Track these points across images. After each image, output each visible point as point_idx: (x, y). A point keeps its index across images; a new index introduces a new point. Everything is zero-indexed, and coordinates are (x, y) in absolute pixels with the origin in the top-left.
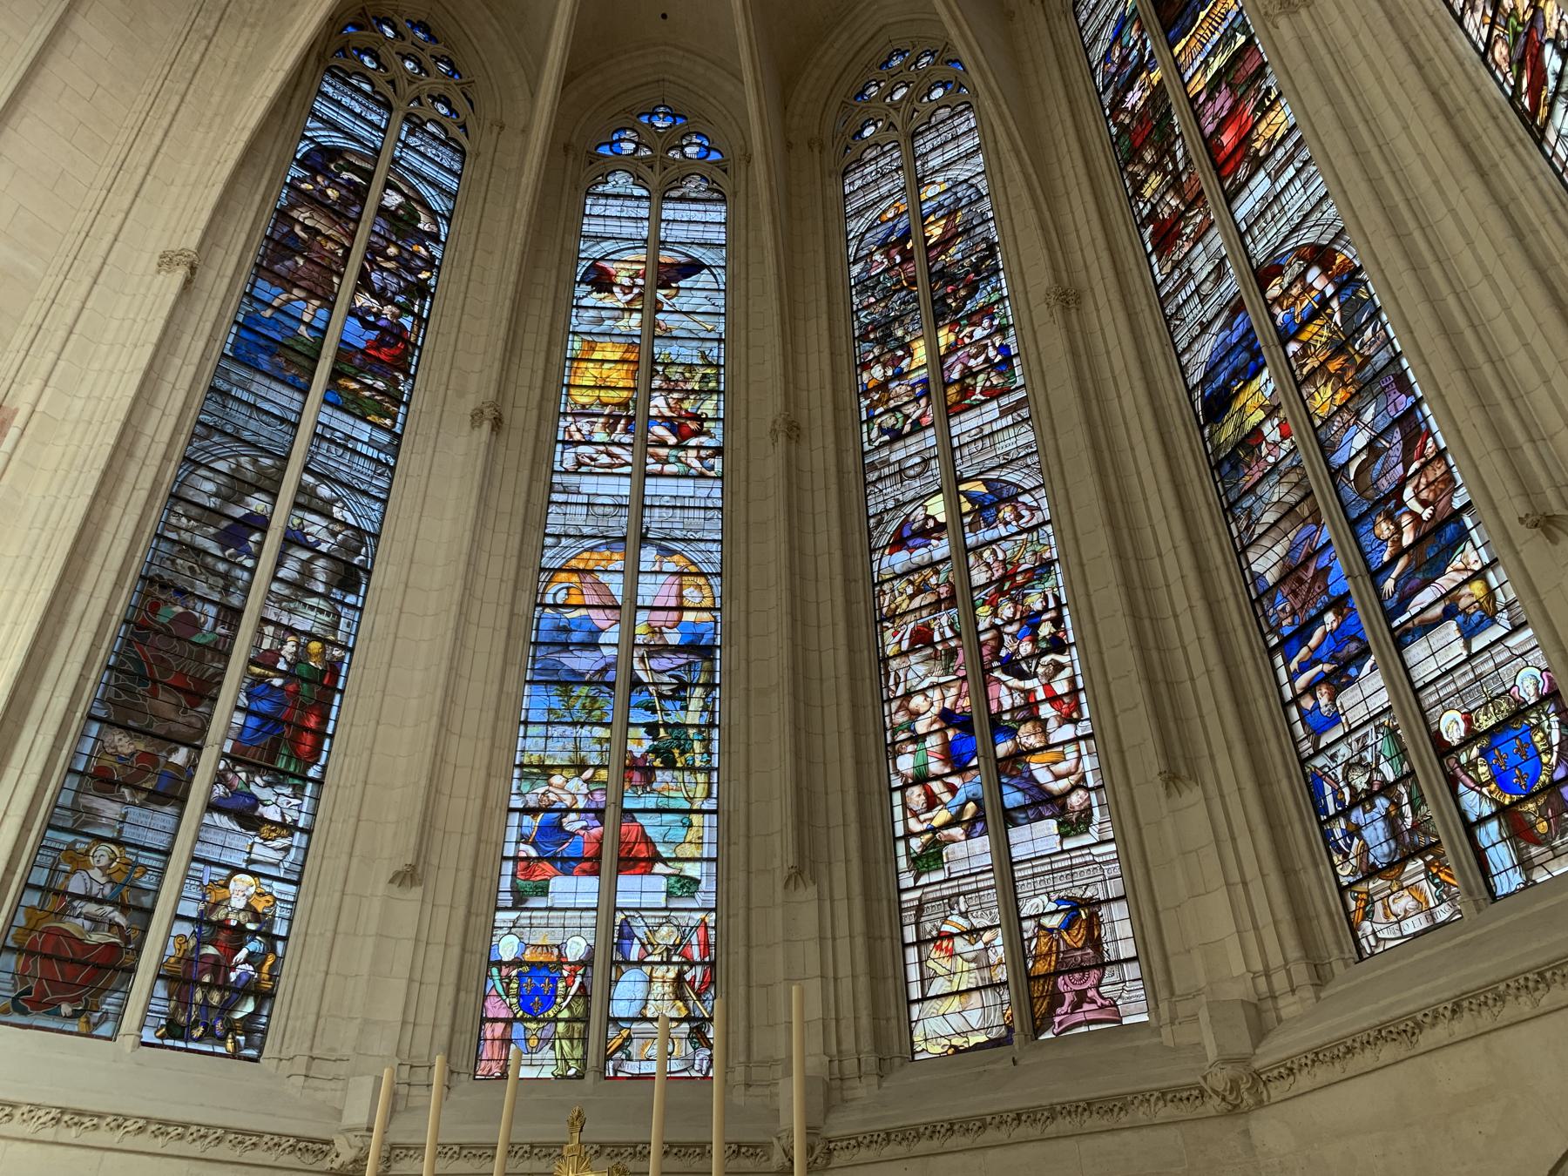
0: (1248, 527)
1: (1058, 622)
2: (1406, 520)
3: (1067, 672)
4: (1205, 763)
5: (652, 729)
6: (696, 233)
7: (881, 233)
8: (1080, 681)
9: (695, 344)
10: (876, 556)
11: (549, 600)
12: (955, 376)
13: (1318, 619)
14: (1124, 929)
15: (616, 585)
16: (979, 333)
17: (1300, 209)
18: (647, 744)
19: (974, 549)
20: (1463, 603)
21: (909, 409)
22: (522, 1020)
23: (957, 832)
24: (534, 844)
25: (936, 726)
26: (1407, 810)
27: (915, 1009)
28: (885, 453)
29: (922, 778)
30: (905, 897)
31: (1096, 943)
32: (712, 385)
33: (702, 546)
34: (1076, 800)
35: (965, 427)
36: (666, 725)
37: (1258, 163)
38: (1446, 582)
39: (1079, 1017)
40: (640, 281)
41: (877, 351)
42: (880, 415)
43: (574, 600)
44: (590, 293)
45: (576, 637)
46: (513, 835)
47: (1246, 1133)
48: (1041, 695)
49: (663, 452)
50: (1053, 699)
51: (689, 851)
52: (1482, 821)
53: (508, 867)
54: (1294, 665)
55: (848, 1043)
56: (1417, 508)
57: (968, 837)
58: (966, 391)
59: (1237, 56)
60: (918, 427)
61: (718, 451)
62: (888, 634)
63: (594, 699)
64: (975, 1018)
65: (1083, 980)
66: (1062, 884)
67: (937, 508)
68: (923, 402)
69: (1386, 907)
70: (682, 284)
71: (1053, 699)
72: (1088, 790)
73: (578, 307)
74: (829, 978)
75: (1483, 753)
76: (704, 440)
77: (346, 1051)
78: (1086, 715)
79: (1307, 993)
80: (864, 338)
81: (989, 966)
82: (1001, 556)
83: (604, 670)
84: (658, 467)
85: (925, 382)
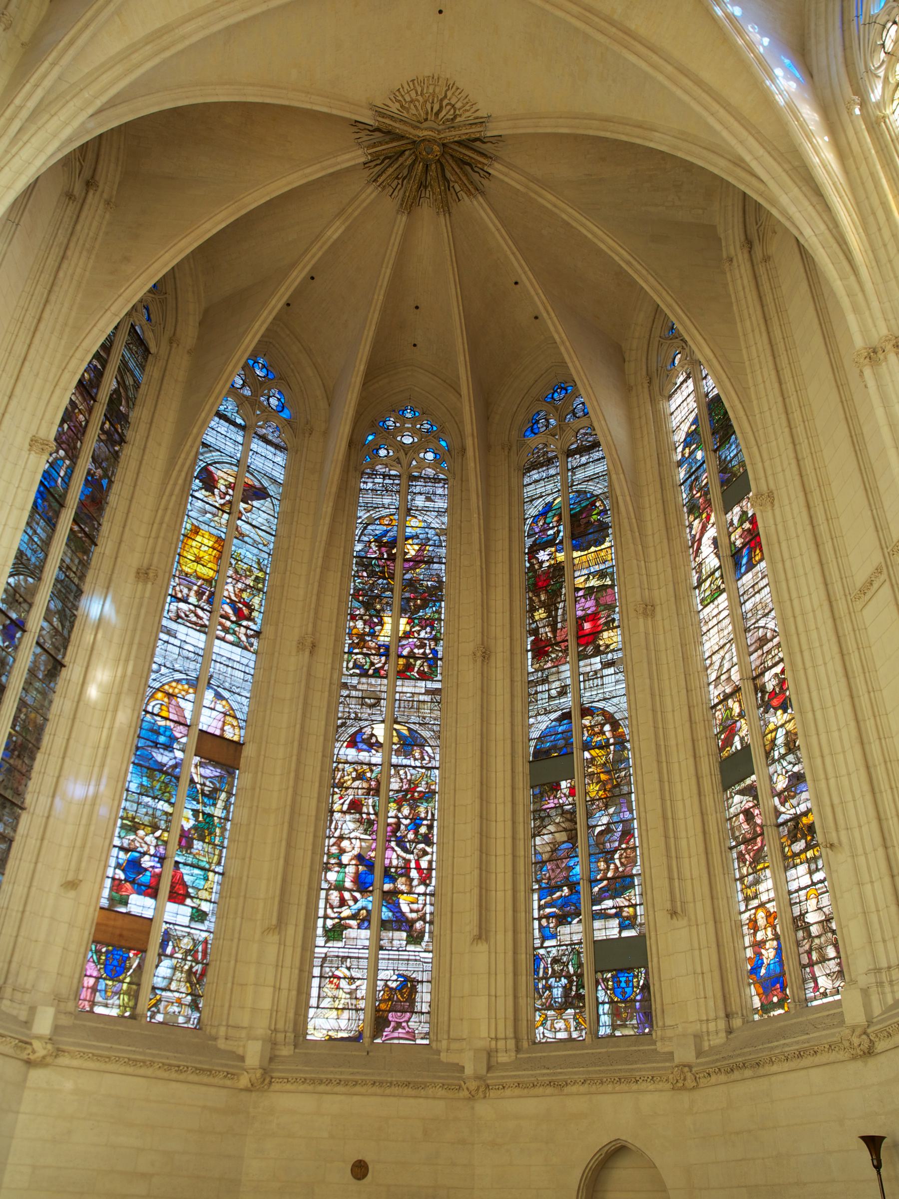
1: (430, 827)
2: (612, 866)
3: (428, 857)
4: (492, 934)
5: (196, 813)
6: (268, 467)
7: (379, 530)
8: (434, 865)
9: (256, 551)
10: (338, 745)
11: (150, 709)
12: (405, 653)
13: (559, 888)
14: (427, 997)
15: (188, 707)
16: (423, 634)
18: (192, 822)
19: (395, 766)
20: (625, 914)
21: (375, 659)
22: (105, 979)
23: (354, 923)
24: (123, 870)
25: (354, 862)
26: (574, 988)
27: (312, 1012)
28: (355, 681)
29: (339, 887)
30: (317, 950)
31: (412, 1002)
32: (260, 586)
33: (239, 698)
34: (418, 925)
35: (405, 689)
36: (204, 813)
37: (597, 652)
38: (621, 902)
39: (396, 1035)
40: (231, 492)
41: (362, 611)
42: (356, 654)
43: (164, 714)
44: (201, 489)
45: (162, 739)
46: (113, 862)
47: (473, 1108)
48: (413, 865)
49: (228, 624)
50: (418, 867)
51: (204, 894)
52: (603, 1003)
53: (108, 883)
54: (542, 902)
55: (280, 1025)
56: (618, 864)
57: (359, 928)
58: (409, 667)
59: (604, 587)
60: (377, 674)
61: (258, 634)
62: (336, 797)
63: (167, 785)
64: (343, 1024)
66: (402, 967)
68: (383, 659)
69: (552, 1024)
70: (255, 503)
71: (418, 867)
72: (425, 922)
73: (193, 496)
74: (277, 989)
75: (613, 976)
76: (250, 624)
77: (28, 986)
78: (433, 883)
79: (513, 1054)
80: (355, 596)
81: (356, 998)
83: (176, 766)
84: (222, 634)
85: (387, 648)
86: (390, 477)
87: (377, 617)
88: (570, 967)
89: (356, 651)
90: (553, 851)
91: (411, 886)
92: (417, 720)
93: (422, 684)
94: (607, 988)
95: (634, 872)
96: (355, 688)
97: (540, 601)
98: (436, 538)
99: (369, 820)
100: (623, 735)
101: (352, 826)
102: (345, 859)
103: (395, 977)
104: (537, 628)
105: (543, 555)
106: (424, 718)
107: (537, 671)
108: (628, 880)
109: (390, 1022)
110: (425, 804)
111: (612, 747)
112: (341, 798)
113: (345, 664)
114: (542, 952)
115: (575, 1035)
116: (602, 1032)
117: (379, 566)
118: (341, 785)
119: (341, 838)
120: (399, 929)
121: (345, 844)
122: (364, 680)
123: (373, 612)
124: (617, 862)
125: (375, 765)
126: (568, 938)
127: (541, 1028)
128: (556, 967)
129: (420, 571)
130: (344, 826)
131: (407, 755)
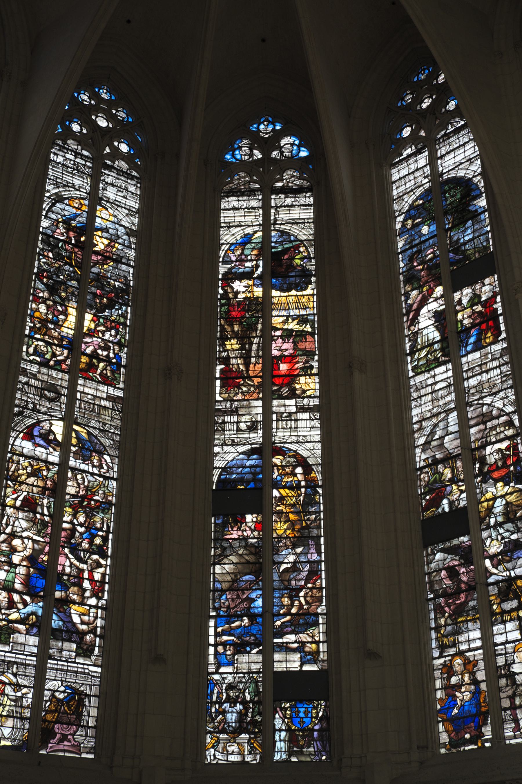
0: (220, 555)
2: (296, 603)
3: (102, 570)
13: (239, 617)
14: (94, 712)
17: (305, 436)
20: (307, 649)
26: (250, 715)
39: (61, 747)
42: (38, 340)
48: (86, 575)
52: (280, 730)
54: (219, 630)
56: (303, 602)
58: (91, 367)
65: (67, 730)
67: (58, 428)
69: (225, 747)
71: (91, 579)
72: (96, 636)
75: (291, 706)
78: (106, 597)
82: (86, 484)
85: (71, 342)
86: (82, 156)
87: (61, 305)
88: (247, 694)
89: (37, 336)
90: (234, 581)
91: (83, 597)
92: (97, 425)
93: (105, 388)
94: (285, 717)
95: (319, 611)
96: (34, 376)
97: (233, 331)
98: (125, 237)
99: (43, 521)
100: (315, 480)
101: (24, 524)
102: (16, 559)
103: (62, 689)
104: (228, 358)
105: (238, 286)
106: (105, 424)
107: (225, 400)
108: (313, 618)
109: (56, 734)
110: (102, 515)
111: (303, 490)
112: (14, 492)
113: (25, 348)
114: (216, 677)
115: (248, 758)
116: (277, 757)
117: (66, 250)
118: (15, 479)
119: (13, 535)
120: (70, 640)
121: (16, 542)
122: (44, 370)
123: (57, 299)
124: (302, 600)
125: (52, 464)
126: (246, 666)
127: (212, 751)
128: (231, 693)
129: (108, 267)
130: (17, 524)
131: (86, 459)
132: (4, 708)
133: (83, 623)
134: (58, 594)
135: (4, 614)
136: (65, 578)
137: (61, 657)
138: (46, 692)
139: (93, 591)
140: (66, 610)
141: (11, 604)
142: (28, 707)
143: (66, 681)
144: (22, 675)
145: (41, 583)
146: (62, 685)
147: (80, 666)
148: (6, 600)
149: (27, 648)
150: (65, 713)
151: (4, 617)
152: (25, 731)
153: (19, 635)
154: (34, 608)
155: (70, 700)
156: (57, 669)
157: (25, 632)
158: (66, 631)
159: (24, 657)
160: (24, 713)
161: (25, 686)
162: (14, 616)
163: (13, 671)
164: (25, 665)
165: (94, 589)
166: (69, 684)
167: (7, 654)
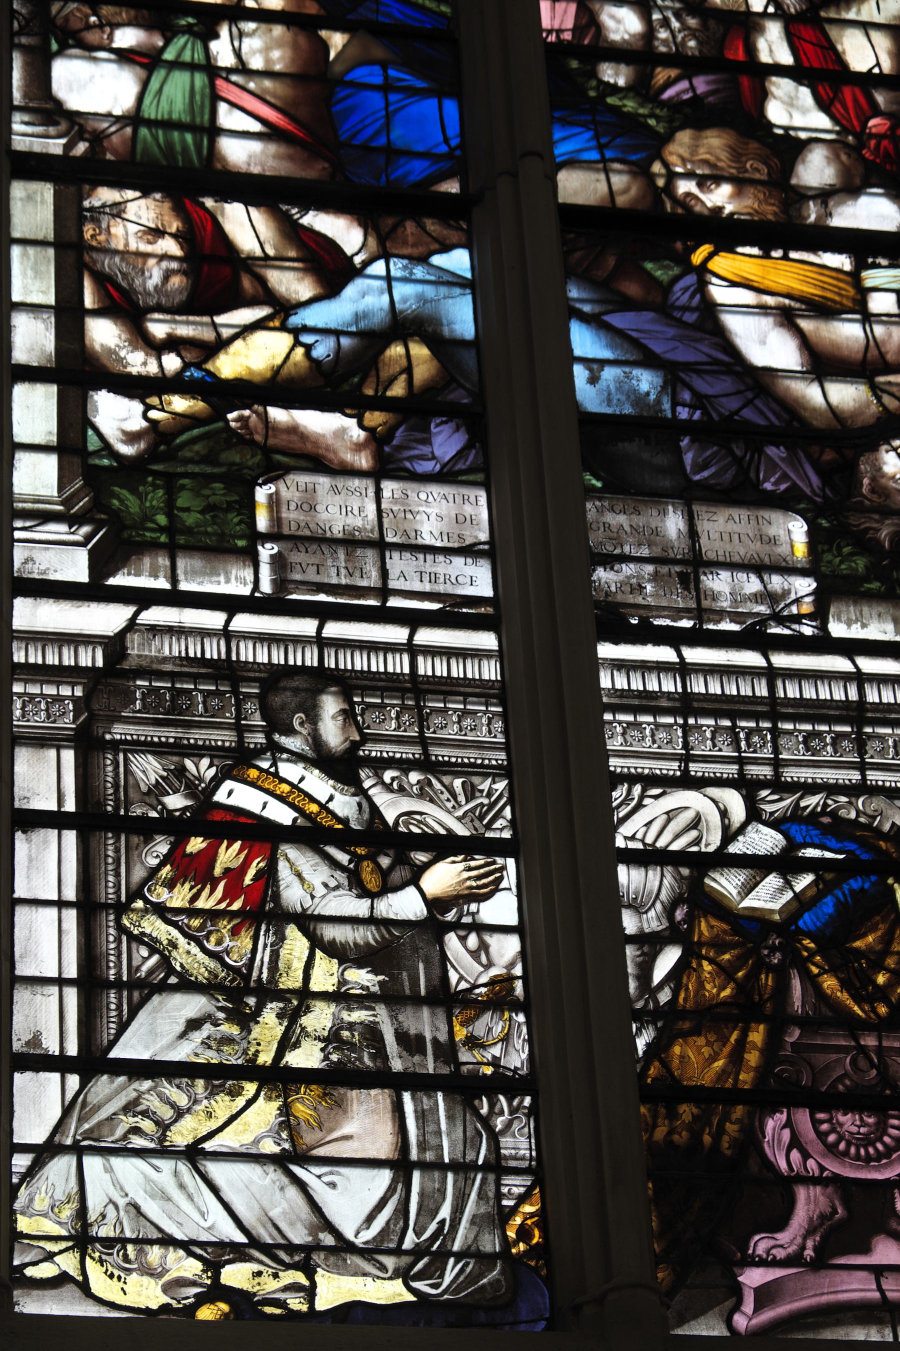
48: (773, 47)
103: (763, 840)
120: (744, 493)
132: (291, 1017)
133: (823, 364)
134: (577, 186)
135: (173, 344)
136: (614, 75)
137: (700, 613)
138: (629, 877)
139: (855, 151)
140: (666, 289)
141: (217, 278)
142: (499, 997)
143: (779, 786)
144: (406, 766)
145: (429, 123)
146: (754, 814)
147: (869, 665)
148: (168, 245)
149: (405, 572)
150: (826, 1016)
151: (172, 363)
152: (515, 1185)
153: (323, 481)
154: (401, 291)
155: (851, 919)
156: (686, 705)
157: (364, 461)
158: (700, 432)
159: (397, 634)
160: (473, 1042)
161: (444, 846)
162: (256, 354)
163: (316, 741)
164: (415, 688)
165: (862, 136)
166: (812, 801)
167: (243, 622)
